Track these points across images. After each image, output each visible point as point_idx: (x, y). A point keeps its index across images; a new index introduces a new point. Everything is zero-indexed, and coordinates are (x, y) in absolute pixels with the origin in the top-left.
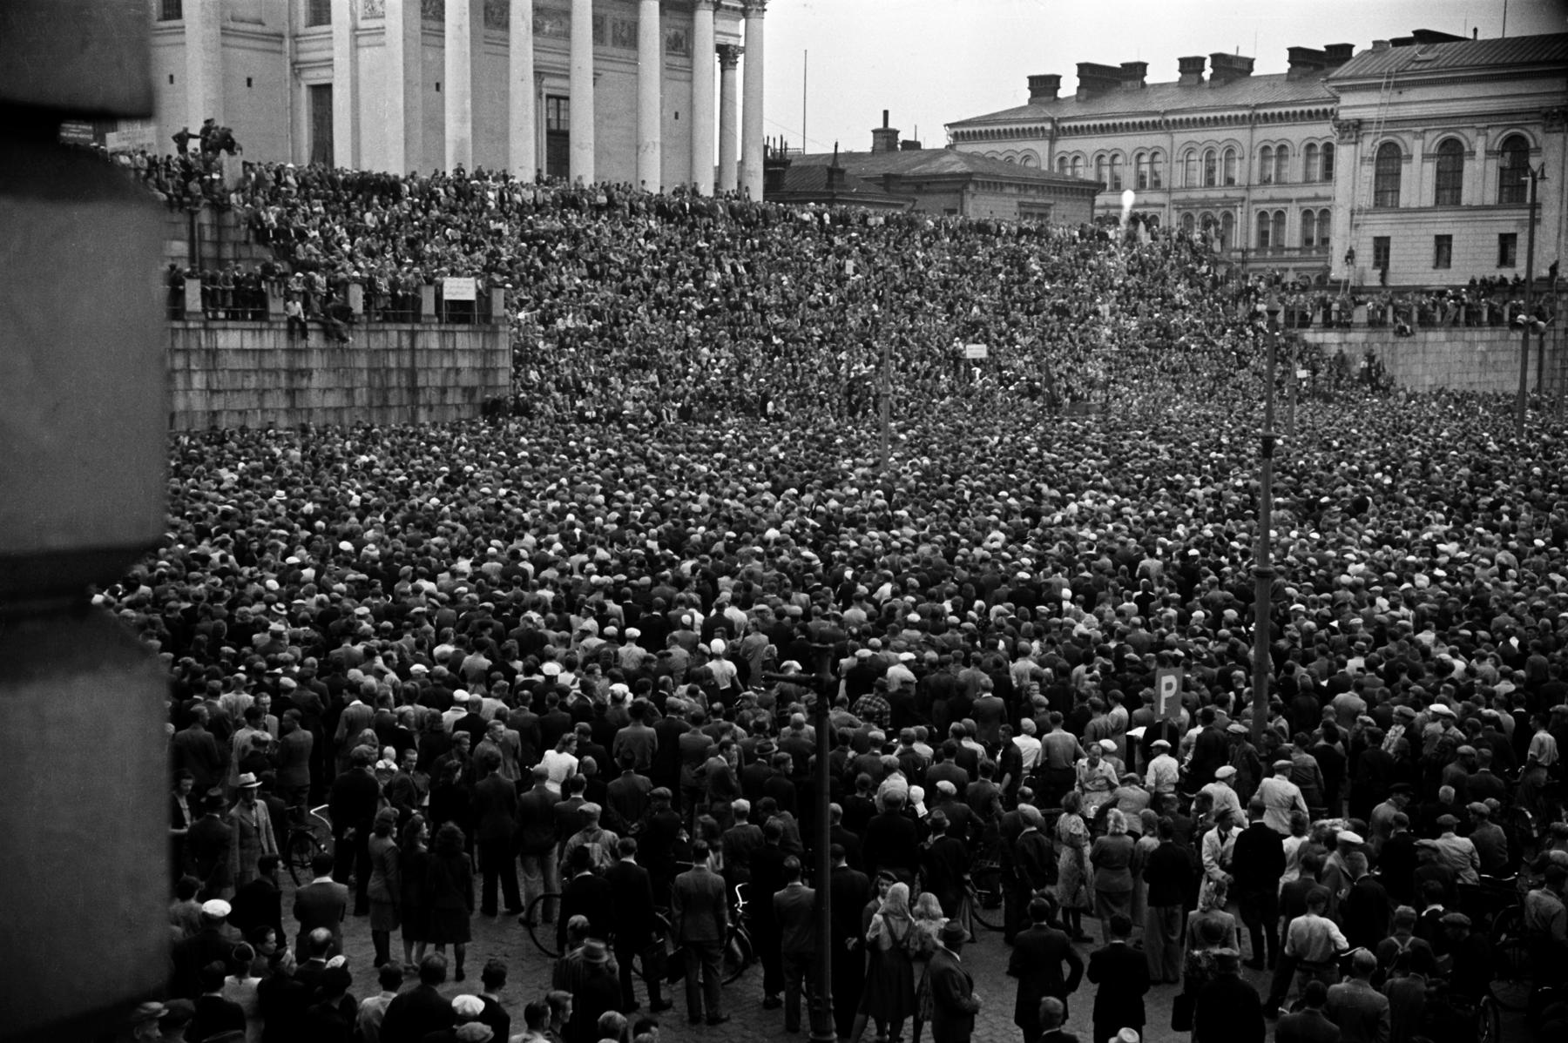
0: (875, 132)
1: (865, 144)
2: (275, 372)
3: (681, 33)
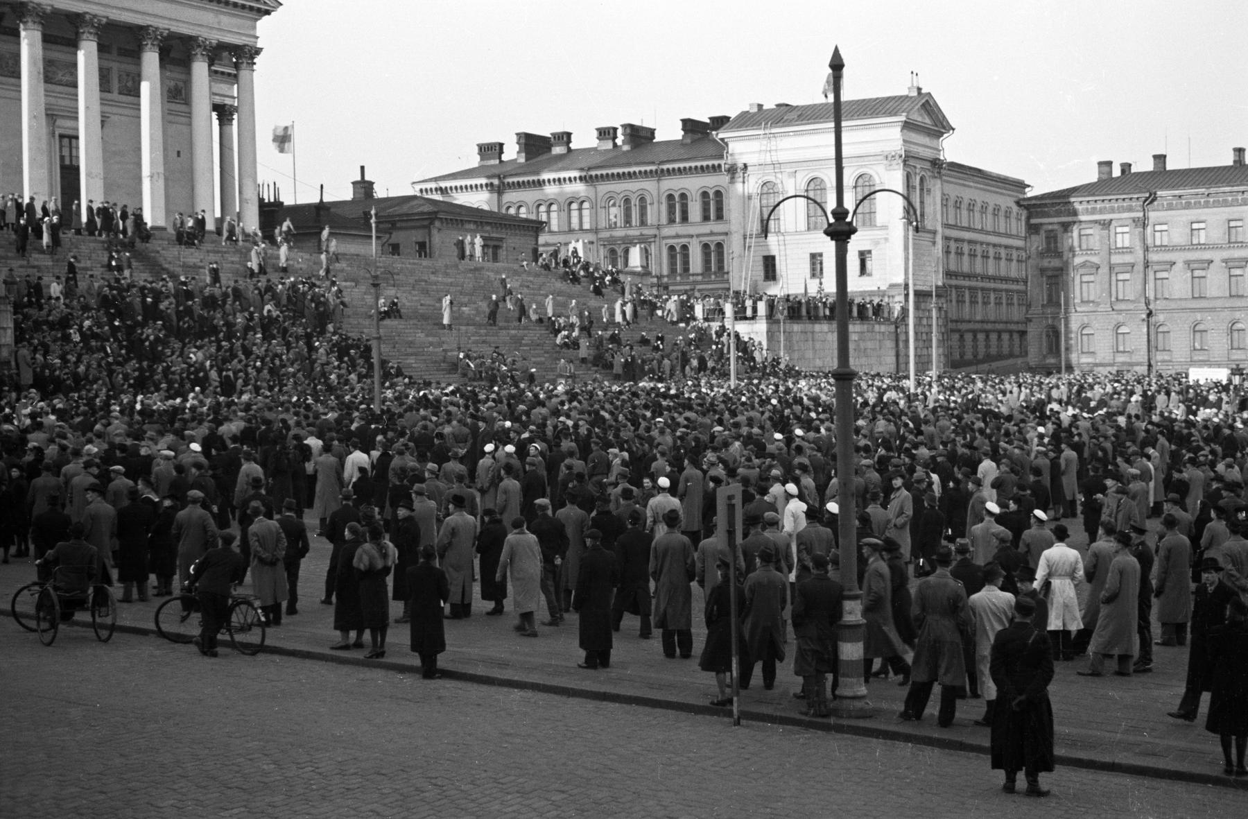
0: (354, 183)
1: (347, 194)
3: (181, 84)
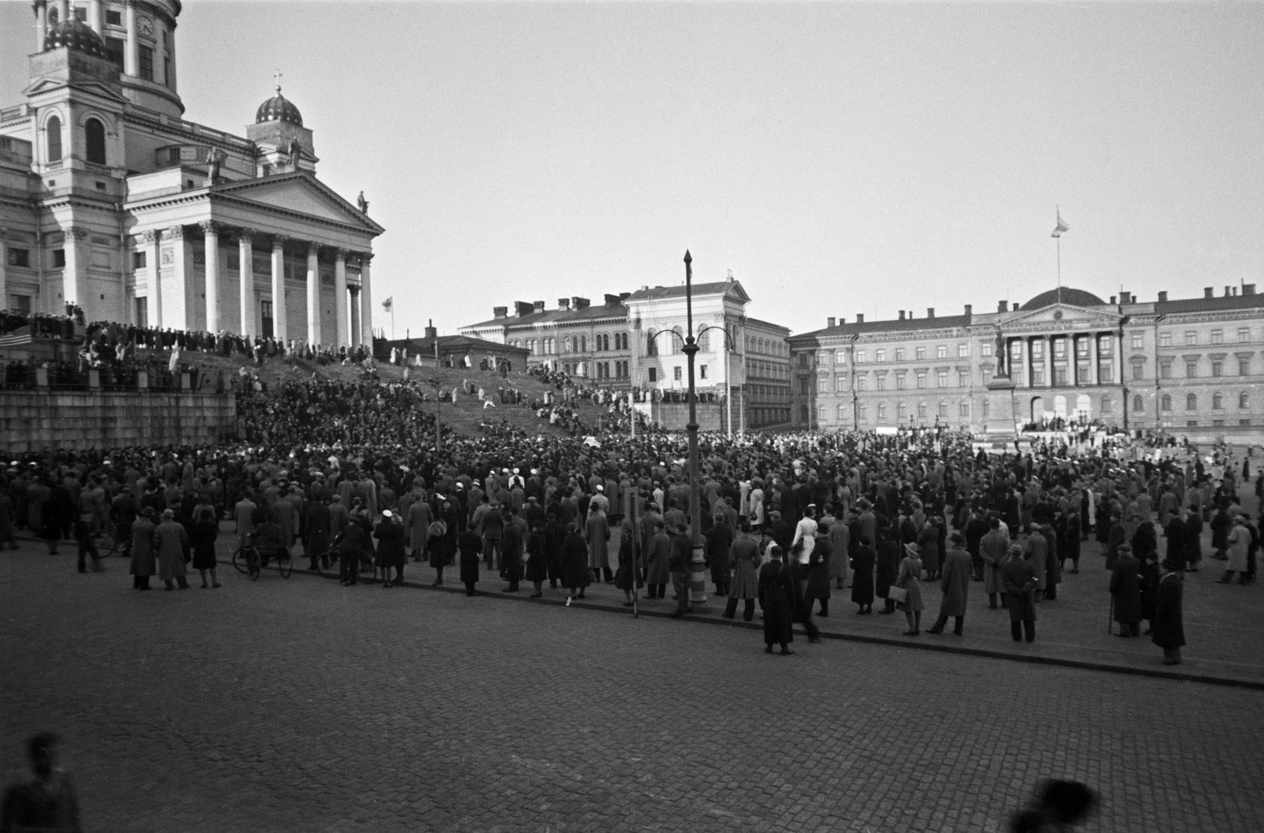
1: (422, 335)
2: (94, 419)
